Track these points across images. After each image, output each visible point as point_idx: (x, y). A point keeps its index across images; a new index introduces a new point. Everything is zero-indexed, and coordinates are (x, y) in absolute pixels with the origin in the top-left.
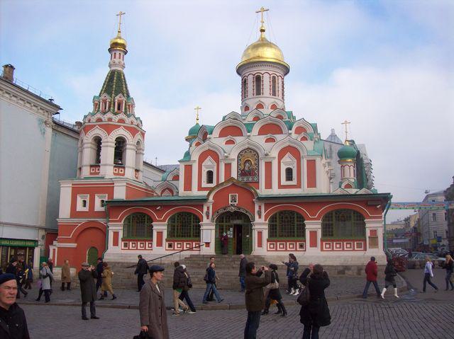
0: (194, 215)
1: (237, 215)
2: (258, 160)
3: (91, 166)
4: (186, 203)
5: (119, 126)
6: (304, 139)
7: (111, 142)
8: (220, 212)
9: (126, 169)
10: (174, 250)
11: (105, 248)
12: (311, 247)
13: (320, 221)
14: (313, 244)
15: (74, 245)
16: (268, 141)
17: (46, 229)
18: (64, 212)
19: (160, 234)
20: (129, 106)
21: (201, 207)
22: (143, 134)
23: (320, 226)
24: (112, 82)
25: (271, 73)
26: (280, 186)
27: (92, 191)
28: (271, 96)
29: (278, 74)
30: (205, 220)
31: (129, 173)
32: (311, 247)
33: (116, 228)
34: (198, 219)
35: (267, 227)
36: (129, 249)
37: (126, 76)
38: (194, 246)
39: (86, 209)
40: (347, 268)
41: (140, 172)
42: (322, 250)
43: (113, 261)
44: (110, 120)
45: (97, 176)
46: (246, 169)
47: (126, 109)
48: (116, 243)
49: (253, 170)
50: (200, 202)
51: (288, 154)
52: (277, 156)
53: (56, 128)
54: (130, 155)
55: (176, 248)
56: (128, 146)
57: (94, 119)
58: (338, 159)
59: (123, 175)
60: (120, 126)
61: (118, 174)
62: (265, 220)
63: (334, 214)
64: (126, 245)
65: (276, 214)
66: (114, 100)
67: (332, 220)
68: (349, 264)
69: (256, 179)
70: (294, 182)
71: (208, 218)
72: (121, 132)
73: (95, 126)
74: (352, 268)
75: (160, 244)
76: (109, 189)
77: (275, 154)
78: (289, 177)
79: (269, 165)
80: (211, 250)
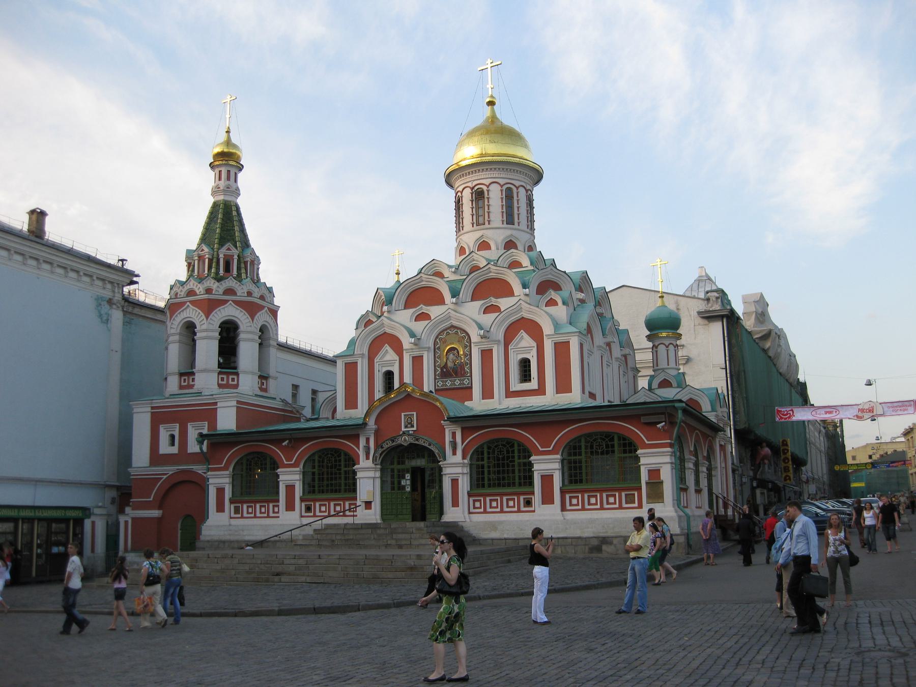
0: (346, 454)
1: (416, 450)
3: (181, 375)
4: (328, 434)
5: (225, 302)
6: (552, 303)
7: (212, 331)
8: (386, 446)
9: (241, 375)
10: (315, 516)
11: (204, 516)
12: (544, 502)
13: (559, 456)
14: (547, 499)
15: (156, 513)
16: (488, 310)
17: (118, 488)
18: (141, 457)
19: (290, 489)
20: (246, 263)
21: (355, 438)
22: (274, 312)
23: (557, 466)
24: (216, 223)
25: (502, 181)
26: (510, 394)
28: (505, 225)
29: (517, 183)
31: (247, 383)
32: (544, 502)
34: (352, 460)
35: (466, 470)
36: (242, 517)
37: (242, 211)
38: (347, 507)
39: (174, 450)
40: (605, 540)
41: (271, 381)
42: (563, 509)
43: (216, 538)
44: (209, 291)
45: (191, 391)
46: (450, 364)
47: (239, 269)
48: (220, 508)
49: (462, 366)
50: (353, 431)
51: (523, 333)
52: (501, 337)
53: (130, 309)
54: (247, 352)
55: (318, 513)
56: (242, 336)
57: (182, 292)
58: (648, 333)
59: (236, 386)
60: (227, 301)
61: (227, 386)
62: (464, 458)
63: (583, 440)
64: (237, 511)
65: (482, 446)
66: (218, 255)
67: (580, 454)
68: (610, 533)
69: (466, 382)
70: (533, 385)
71: (368, 458)
72: (228, 312)
73: (183, 304)
74: (615, 541)
75: (290, 507)
76: (209, 413)
77: (499, 334)
78: (525, 376)
79: (486, 355)
80: (373, 516)
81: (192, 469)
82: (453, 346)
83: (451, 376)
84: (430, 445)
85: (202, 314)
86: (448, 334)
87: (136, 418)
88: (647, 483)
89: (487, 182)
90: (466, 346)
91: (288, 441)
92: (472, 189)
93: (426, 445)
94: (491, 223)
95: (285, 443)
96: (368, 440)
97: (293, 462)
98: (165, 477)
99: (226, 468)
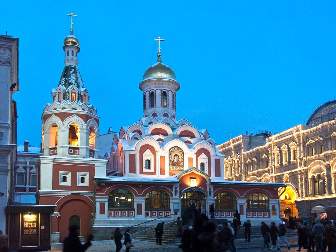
2: (183, 155)
25: (173, 91)
27: (74, 169)
30: (174, 197)
33: (102, 200)
46: (175, 161)
64: (109, 215)
71: (176, 195)
73: (73, 114)
76: (91, 169)
81: (81, 194)
82: (176, 154)
83: (176, 165)
84: (204, 192)
85: (82, 120)
86: (175, 149)
87: (42, 167)
88: (272, 210)
89: (168, 89)
90: (182, 155)
91: (141, 185)
92: (161, 91)
93: (203, 192)
94: (169, 106)
95: (140, 186)
96: (176, 188)
97: (142, 194)
98: (63, 197)
99: (105, 195)
